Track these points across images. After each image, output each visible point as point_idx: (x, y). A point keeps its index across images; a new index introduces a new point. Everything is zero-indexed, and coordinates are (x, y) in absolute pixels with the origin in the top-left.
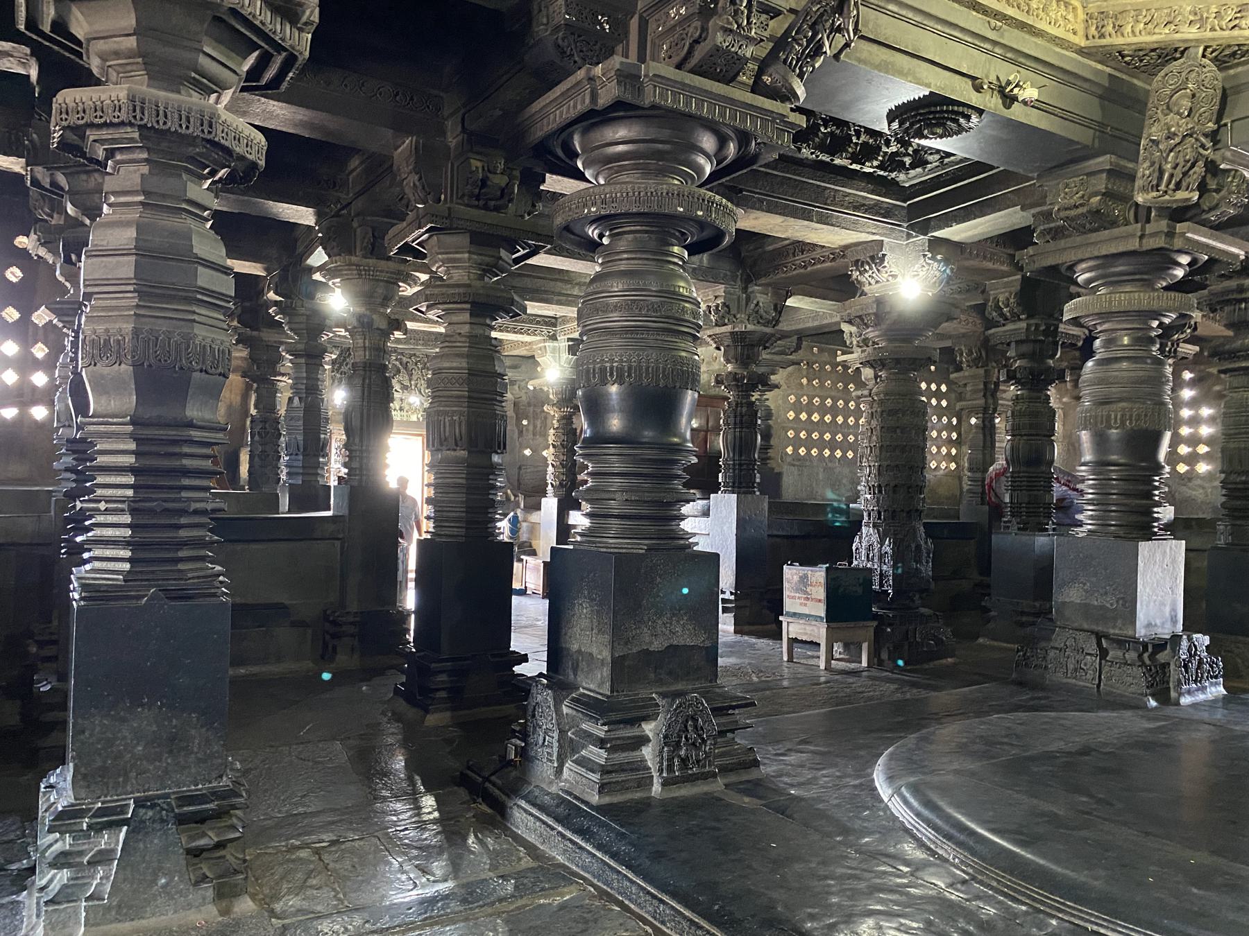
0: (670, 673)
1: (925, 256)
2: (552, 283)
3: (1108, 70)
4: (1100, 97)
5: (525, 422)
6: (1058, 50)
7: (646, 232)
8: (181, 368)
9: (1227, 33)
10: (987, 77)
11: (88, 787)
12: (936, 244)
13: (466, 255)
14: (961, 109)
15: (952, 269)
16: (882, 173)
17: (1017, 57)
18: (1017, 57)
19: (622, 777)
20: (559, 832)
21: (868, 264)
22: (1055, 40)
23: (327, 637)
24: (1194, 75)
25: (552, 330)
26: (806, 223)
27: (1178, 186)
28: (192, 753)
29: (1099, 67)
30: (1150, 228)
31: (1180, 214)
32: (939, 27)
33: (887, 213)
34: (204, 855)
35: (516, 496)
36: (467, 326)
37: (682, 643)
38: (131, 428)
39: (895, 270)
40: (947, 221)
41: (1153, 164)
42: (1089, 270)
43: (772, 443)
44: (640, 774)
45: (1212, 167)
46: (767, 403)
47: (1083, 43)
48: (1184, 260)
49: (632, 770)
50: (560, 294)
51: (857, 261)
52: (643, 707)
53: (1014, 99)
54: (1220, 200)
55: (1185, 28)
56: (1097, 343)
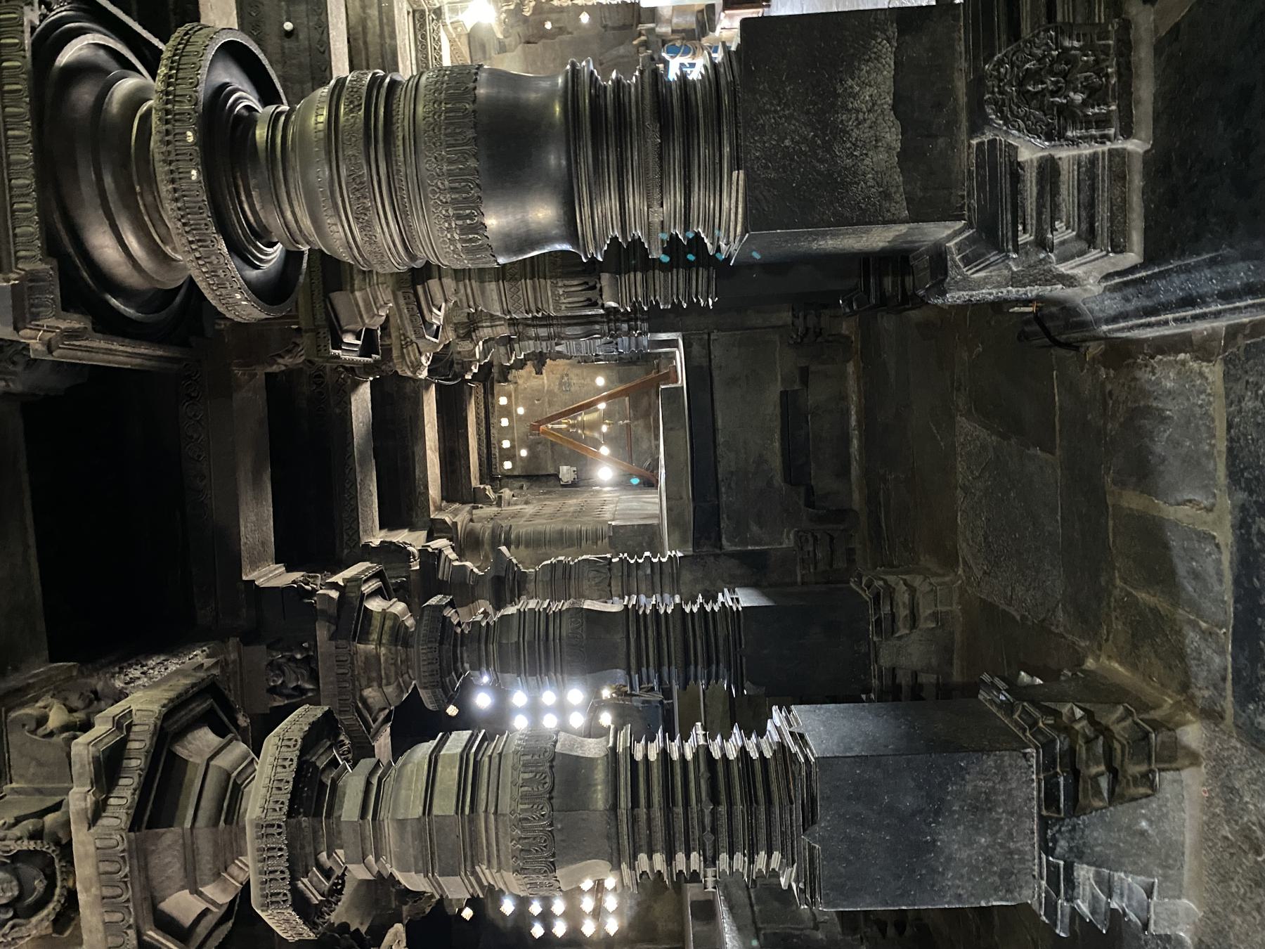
0: (939, 106)
2: (371, 49)
5: (548, 26)
7: (249, 196)
8: (551, 825)
11: (1021, 887)
13: (358, 294)
19: (1103, 212)
20: (1175, 320)
23: (819, 339)
25: (430, 17)
28: (993, 787)
34: (1117, 764)
35: (640, 34)
36: (444, 280)
37: (890, 83)
38: (624, 866)
44: (1102, 171)
49: (1093, 188)
50: (382, 35)
52: (993, 169)
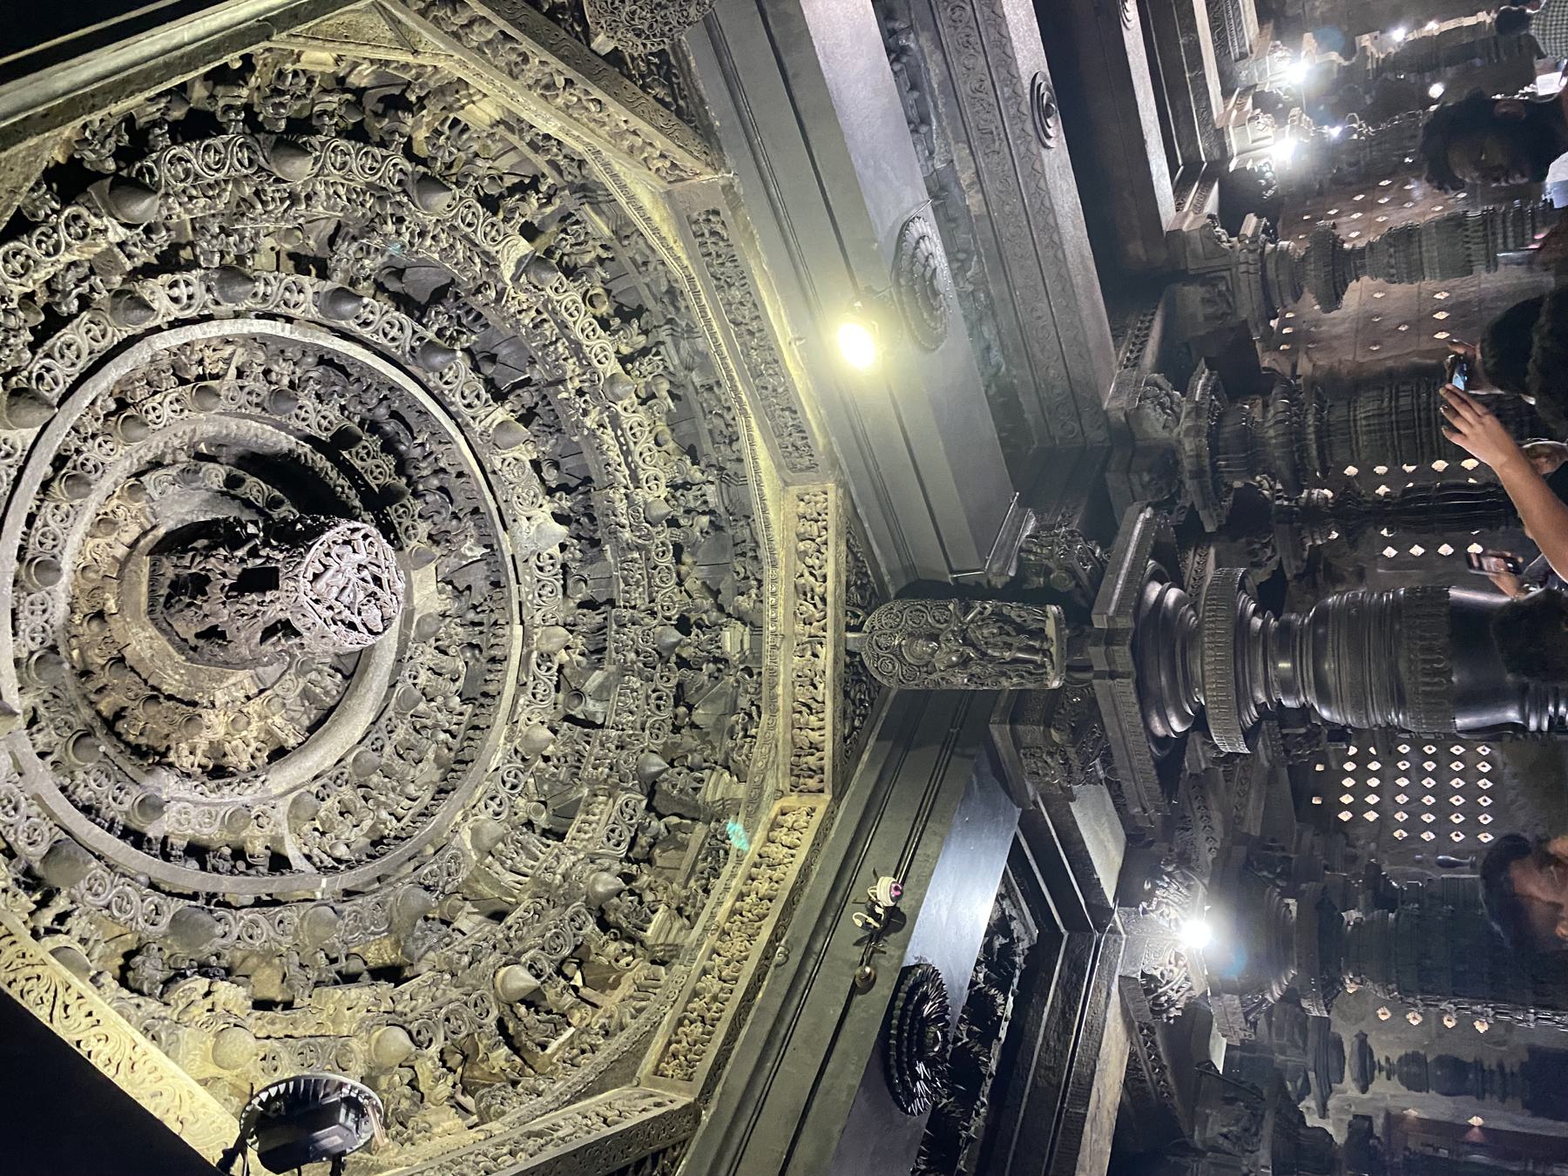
1: (1145, 911)
3: (871, 742)
4: (907, 749)
6: (832, 834)
9: (830, 611)
10: (853, 966)
12: (1127, 894)
14: (897, 1012)
15: (1168, 863)
16: (1016, 981)
17: (834, 906)
18: (834, 906)
21: (1159, 996)
22: (816, 846)
24: (882, 640)
26: (1087, 1127)
27: (1040, 633)
29: (865, 757)
30: (1101, 666)
31: (1077, 616)
32: (769, 1065)
33: (1076, 969)
39: (1168, 956)
40: (1090, 883)
41: (1004, 674)
42: (1165, 722)
43: (1470, 1060)
45: (1015, 591)
46: (1394, 1060)
47: (827, 796)
48: (1154, 590)
51: (1152, 1011)
53: (893, 912)
54: (1060, 567)
55: (820, 663)
56: (1288, 703)
